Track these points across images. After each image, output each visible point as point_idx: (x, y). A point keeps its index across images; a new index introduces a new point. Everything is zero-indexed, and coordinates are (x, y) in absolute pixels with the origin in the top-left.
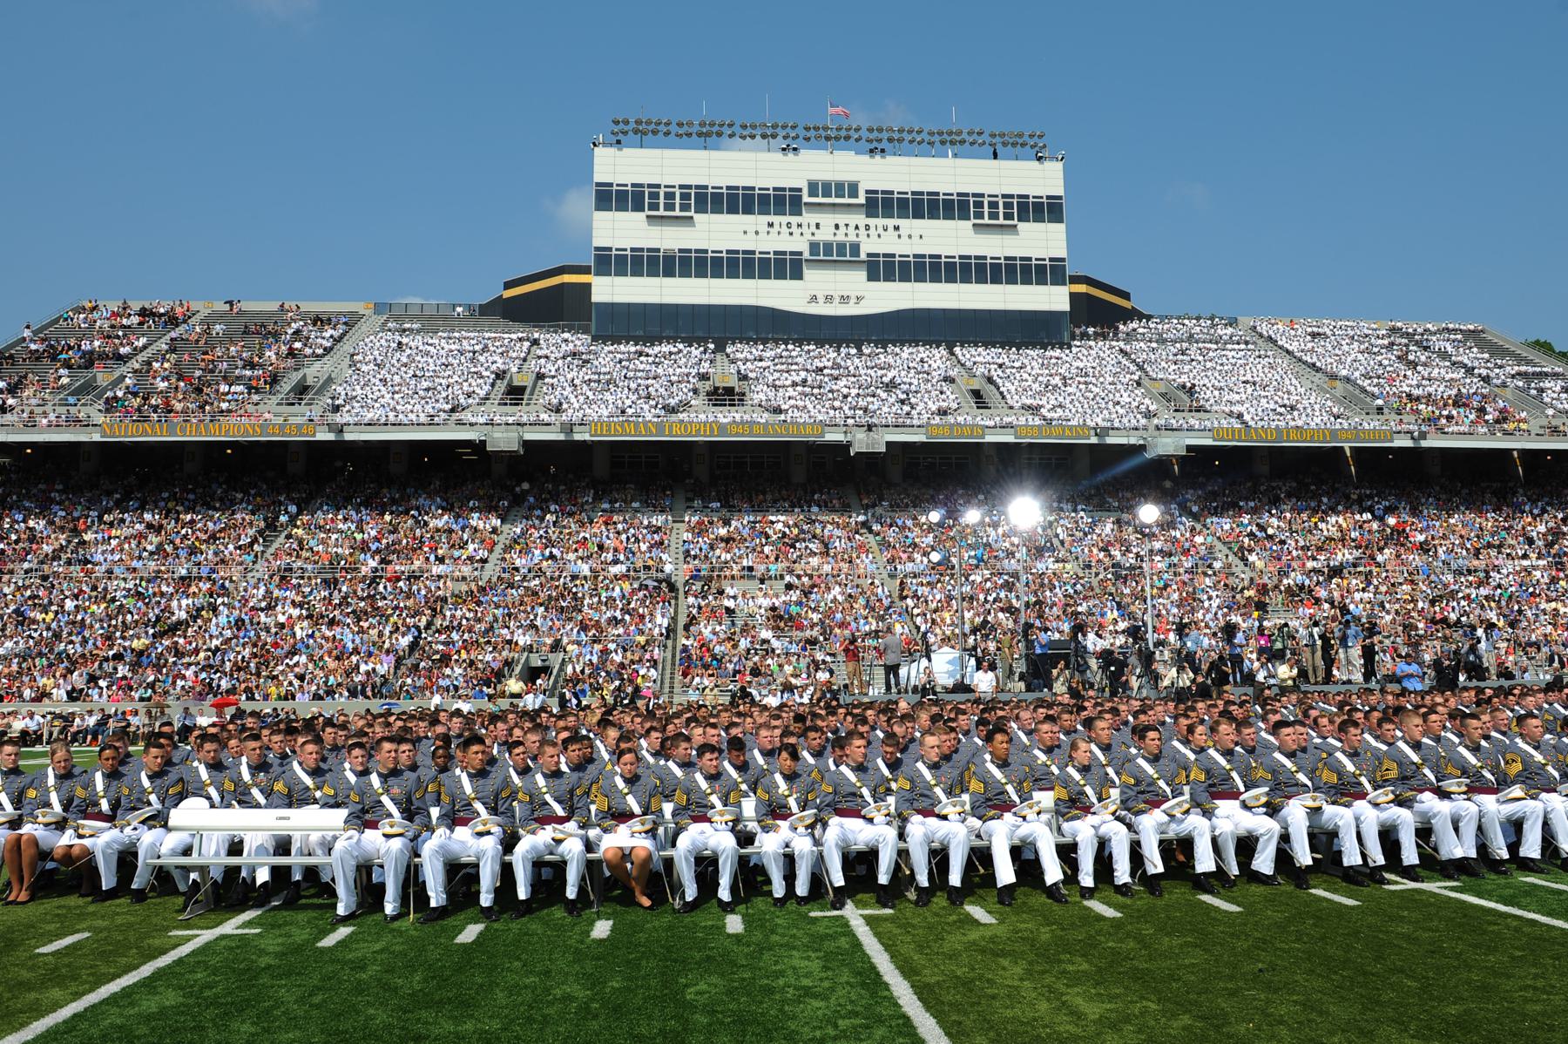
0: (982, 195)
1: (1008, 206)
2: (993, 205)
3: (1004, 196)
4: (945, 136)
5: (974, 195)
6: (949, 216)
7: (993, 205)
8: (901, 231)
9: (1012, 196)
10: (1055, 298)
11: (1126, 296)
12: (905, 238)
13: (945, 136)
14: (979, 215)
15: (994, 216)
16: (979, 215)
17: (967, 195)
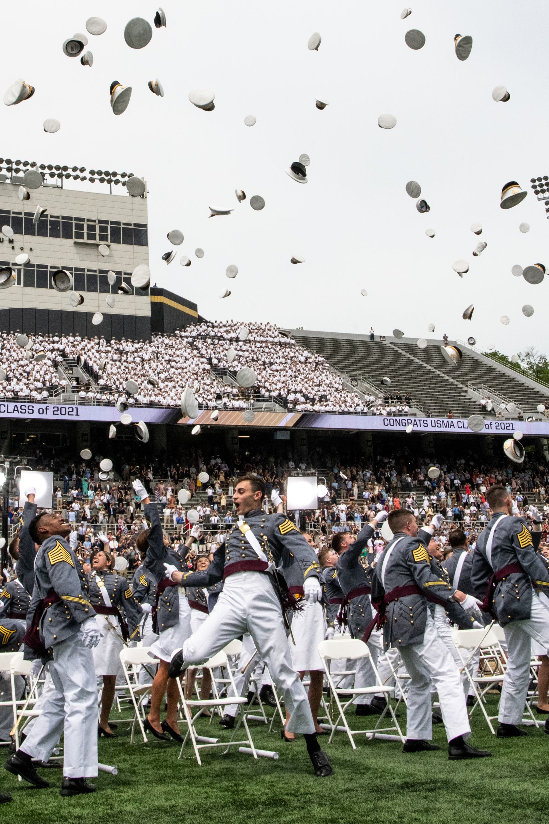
0: (82, 220)
1: (103, 229)
2: (91, 228)
3: (100, 222)
4: (54, 170)
5: (76, 219)
6: (55, 234)
7: (91, 228)
8: (15, 244)
9: (106, 222)
10: (141, 307)
11: (194, 307)
12: (17, 249)
13: (54, 170)
14: (80, 236)
15: (91, 237)
16: (80, 236)
17: (70, 218)
